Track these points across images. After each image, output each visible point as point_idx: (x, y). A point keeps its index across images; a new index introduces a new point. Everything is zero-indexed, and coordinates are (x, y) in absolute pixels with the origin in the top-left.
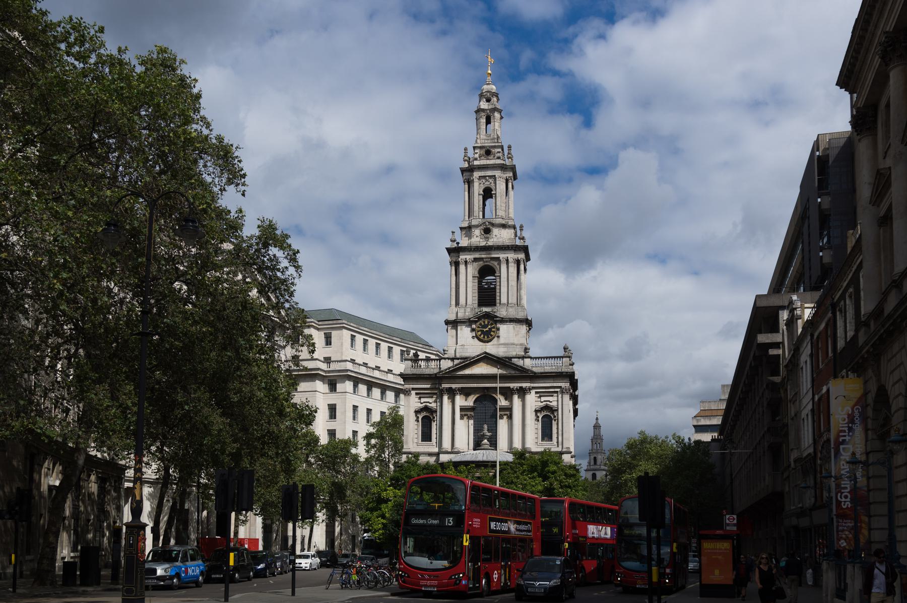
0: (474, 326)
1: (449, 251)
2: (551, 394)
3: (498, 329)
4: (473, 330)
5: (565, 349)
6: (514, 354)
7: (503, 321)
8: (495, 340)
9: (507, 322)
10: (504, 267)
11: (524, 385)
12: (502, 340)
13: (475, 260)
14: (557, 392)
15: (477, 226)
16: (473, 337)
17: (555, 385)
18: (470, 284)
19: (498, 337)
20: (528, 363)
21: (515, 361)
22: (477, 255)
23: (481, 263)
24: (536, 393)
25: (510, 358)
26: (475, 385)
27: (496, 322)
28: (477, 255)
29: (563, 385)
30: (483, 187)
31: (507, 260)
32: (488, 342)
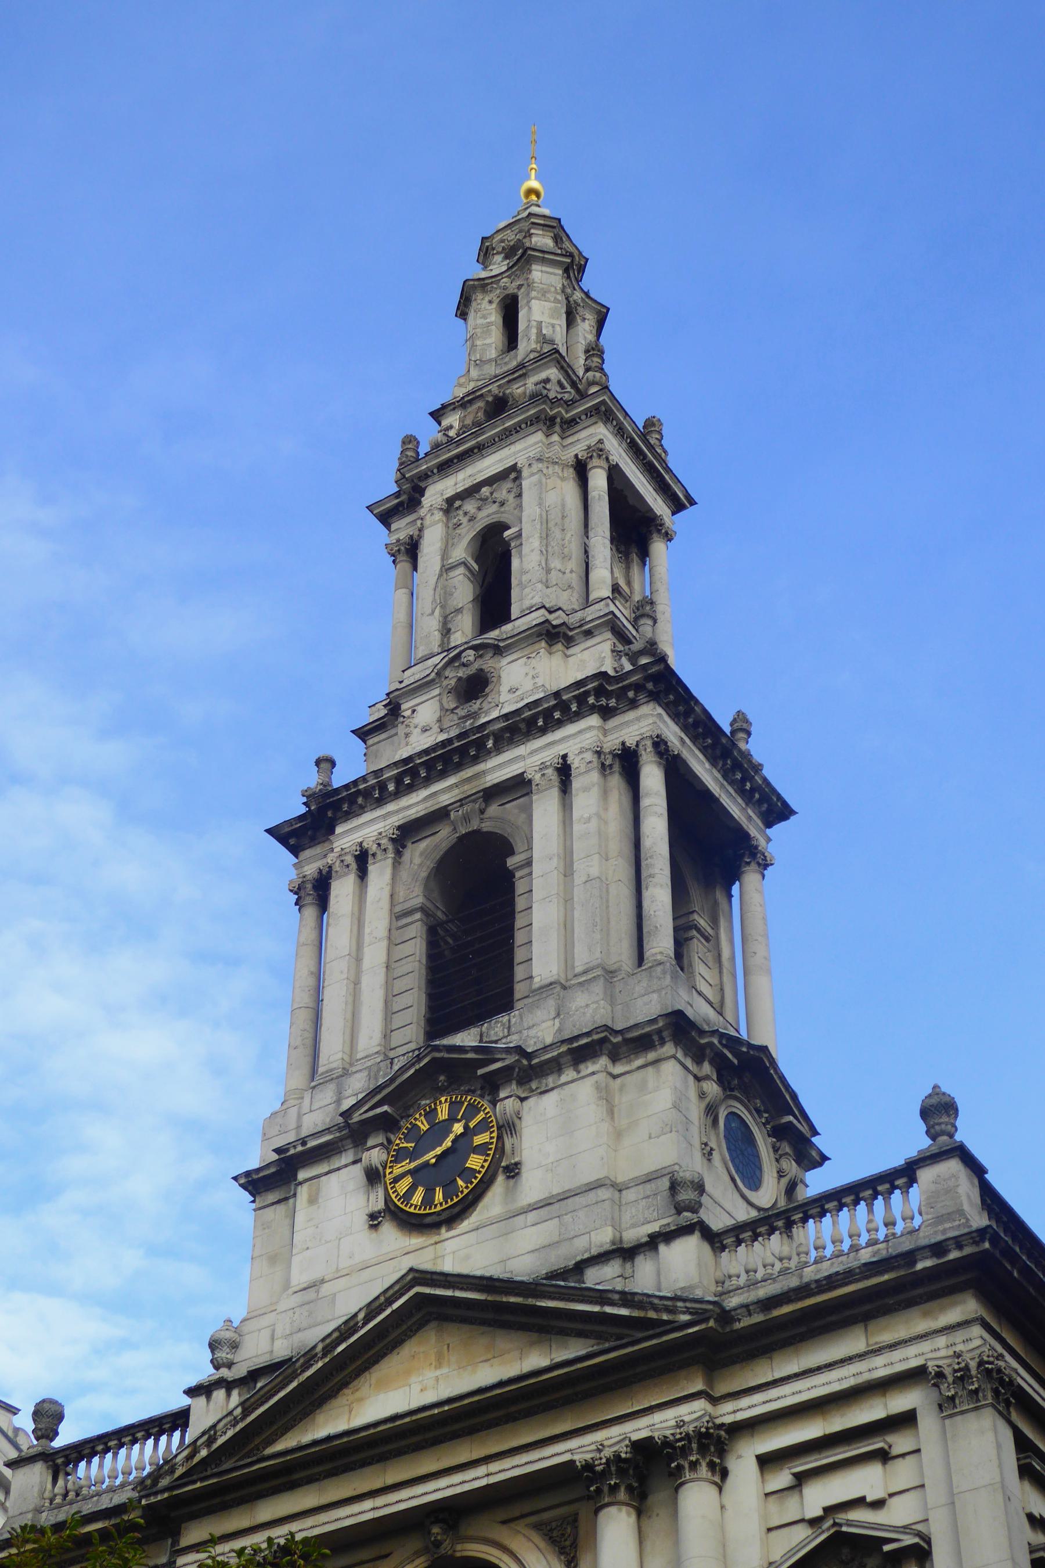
0: (375, 1156)
1: (295, 836)
2: (871, 1444)
3: (508, 1127)
4: (373, 1176)
5: (938, 1111)
6: (603, 1238)
7: (531, 1071)
8: (493, 1203)
9: (555, 1066)
10: (545, 811)
11: (662, 1424)
12: (533, 1185)
13: (407, 833)
14: (907, 1420)
15: (422, 686)
16: (374, 1220)
17: (881, 1367)
18: (375, 955)
19: (513, 1171)
20: (682, 1268)
21: (603, 1277)
22: (414, 804)
23: (443, 837)
24: (767, 1462)
25: (580, 1267)
26: (365, 1511)
27: (491, 1086)
28: (414, 804)
29: (932, 1353)
30: (468, 533)
31: (564, 771)
32: (453, 1217)
